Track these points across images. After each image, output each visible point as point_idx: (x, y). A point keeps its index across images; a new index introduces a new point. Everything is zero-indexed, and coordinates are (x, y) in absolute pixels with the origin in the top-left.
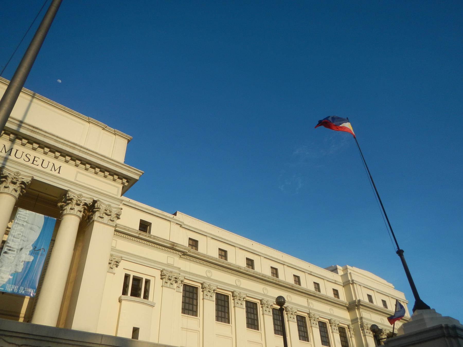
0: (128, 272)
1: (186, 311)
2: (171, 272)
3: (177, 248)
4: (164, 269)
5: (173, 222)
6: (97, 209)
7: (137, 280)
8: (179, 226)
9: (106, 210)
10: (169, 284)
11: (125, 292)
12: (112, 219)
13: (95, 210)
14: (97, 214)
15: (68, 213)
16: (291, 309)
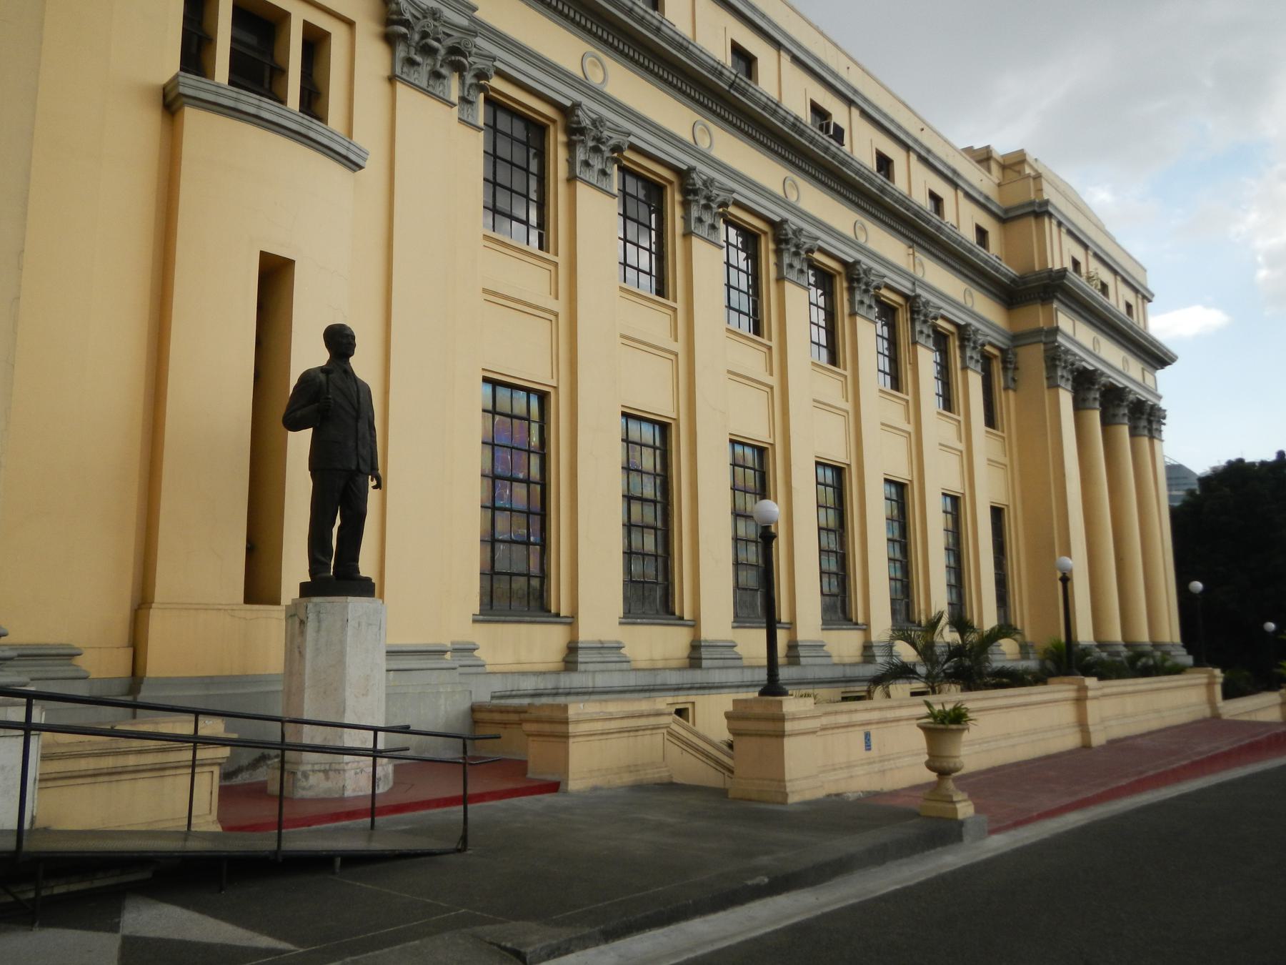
10: (425, 70)
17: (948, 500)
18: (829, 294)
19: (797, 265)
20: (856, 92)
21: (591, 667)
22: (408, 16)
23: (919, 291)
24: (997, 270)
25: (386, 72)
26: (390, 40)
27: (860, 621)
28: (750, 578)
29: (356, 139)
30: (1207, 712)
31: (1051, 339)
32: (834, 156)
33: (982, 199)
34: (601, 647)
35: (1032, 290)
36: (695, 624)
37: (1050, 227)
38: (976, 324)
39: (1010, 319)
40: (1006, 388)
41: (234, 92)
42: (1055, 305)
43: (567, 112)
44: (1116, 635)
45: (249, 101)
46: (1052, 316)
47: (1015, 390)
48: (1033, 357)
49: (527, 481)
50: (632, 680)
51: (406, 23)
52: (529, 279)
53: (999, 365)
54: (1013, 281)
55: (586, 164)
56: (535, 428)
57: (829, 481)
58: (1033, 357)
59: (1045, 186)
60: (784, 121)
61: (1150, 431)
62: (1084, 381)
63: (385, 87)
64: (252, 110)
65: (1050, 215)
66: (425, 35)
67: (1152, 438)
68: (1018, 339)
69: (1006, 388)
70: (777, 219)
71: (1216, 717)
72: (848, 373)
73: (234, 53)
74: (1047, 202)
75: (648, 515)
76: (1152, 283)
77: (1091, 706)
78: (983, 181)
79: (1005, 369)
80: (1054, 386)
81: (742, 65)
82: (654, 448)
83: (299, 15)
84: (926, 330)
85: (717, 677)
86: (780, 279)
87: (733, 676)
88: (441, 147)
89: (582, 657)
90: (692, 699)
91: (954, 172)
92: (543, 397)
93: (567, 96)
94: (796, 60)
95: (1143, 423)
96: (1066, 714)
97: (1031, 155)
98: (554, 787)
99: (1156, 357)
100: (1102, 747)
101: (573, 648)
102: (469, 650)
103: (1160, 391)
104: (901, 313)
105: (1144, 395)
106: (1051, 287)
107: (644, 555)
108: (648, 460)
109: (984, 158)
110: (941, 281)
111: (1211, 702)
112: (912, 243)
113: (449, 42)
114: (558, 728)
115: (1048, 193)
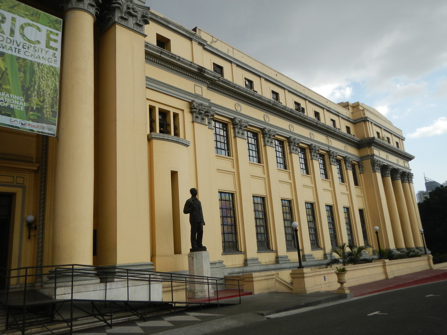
0: (153, 104)
1: (219, 150)
2: (201, 105)
3: (205, 74)
4: (194, 101)
5: (196, 41)
6: (117, 5)
7: (164, 114)
8: (201, 48)
9: (128, 8)
10: (200, 118)
11: (152, 129)
12: (138, 22)
13: (113, 5)
15: (74, 6)
16: (315, 147)
17: (345, 209)
18: (305, 154)
19: (295, 148)
20: (307, 96)
21: (251, 265)
22: (196, 107)
23: (330, 149)
24: (353, 139)
25: (191, 120)
26: (192, 113)
27: (322, 247)
28: (290, 237)
29: (187, 139)
30: (428, 268)
31: (372, 158)
33: (347, 119)
34: (253, 260)
36: (276, 252)
37: (369, 125)
38: (348, 156)
40: (360, 173)
41: (162, 134)
43: (233, 120)
44: (403, 246)
45: (166, 136)
46: (372, 151)
47: (363, 174)
48: (367, 163)
49: (231, 217)
50: (262, 268)
51: (195, 108)
52: (226, 164)
53: (357, 167)
54: (359, 141)
55: (238, 132)
56: (231, 202)
57: (309, 207)
58: (367, 163)
60: (288, 111)
61: (408, 180)
62: (384, 169)
63: (191, 124)
64: (167, 138)
65: (368, 121)
66: (199, 110)
67: (409, 183)
69: (360, 173)
70: (288, 137)
71: (431, 269)
72: (312, 176)
73: (160, 123)
74: (367, 117)
75: (261, 222)
77: (388, 268)
79: (359, 167)
80: (374, 171)
81: (275, 95)
82: (261, 204)
83: (172, 111)
84: (334, 160)
85: (284, 266)
86: (291, 153)
87: (288, 265)
88: (204, 136)
89: (248, 262)
90: (277, 272)
91: (338, 112)
92: (232, 194)
93: (232, 116)
94: (289, 91)
96: (381, 270)
97: (361, 102)
98: (251, 293)
99: (408, 158)
100: (392, 279)
101: (246, 260)
102: (221, 262)
103: (410, 168)
104: (327, 157)
105: (405, 170)
106: (371, 142)
107: (261, 234)
108: (260, 208)
109: (346, 105)
110: (336, 144)
111: (430, 265)
112: (327, 136)
113: (205, 110)
114: (251, 279)
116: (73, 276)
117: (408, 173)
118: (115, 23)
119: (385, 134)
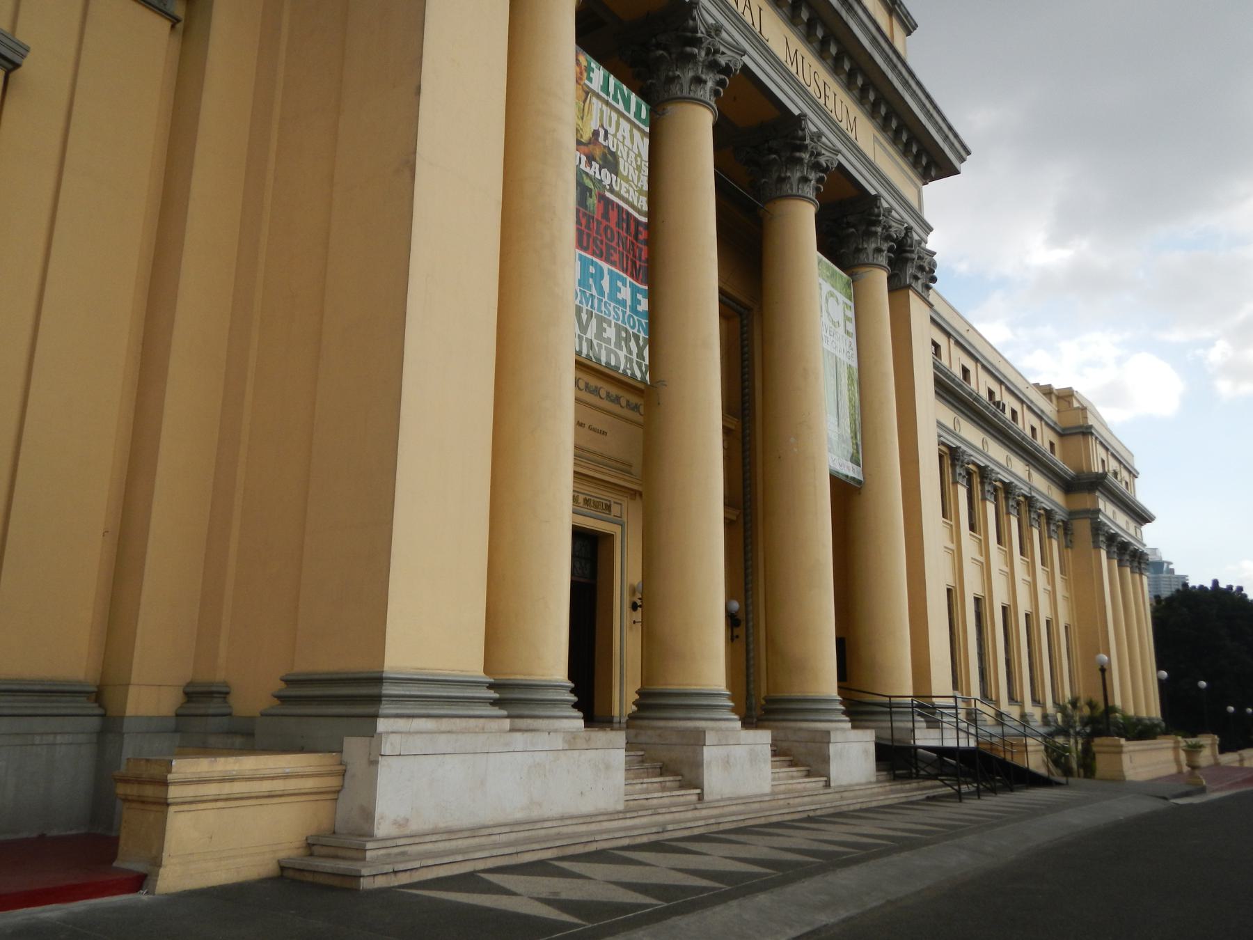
13: (909, 255)
14: (910, 270)
32: (1000, 419)
35: (1084, 484)
39: (1067, 502)
40: (1067, 547)
42: (1097, 494)
59: (1089, 415)
62: (1112, 539)
65: (1092, 434)
68: (1073, 515)
71: (1217, 764)
74: (1091, 427)
76: (1138, 465)
78: (1048, 408)
80: (1097, 547)
95: (1136, 564)
96: (1169, 755)
97: (1075, 389)
99: (1142, 517)
105: (1137, 546)
109: (1048, 392)
112: (1028, 463)
115: (1091, 421)
116: (891, 713)
117: (1136, 550)
118: (910, 286)
119: (1113, 465)
